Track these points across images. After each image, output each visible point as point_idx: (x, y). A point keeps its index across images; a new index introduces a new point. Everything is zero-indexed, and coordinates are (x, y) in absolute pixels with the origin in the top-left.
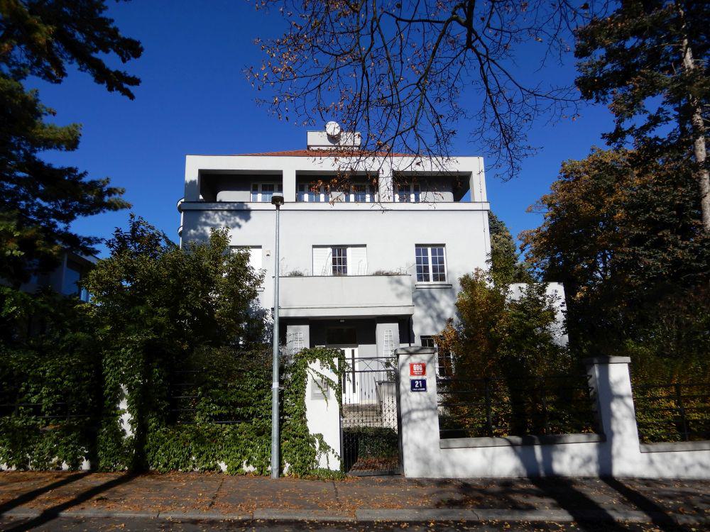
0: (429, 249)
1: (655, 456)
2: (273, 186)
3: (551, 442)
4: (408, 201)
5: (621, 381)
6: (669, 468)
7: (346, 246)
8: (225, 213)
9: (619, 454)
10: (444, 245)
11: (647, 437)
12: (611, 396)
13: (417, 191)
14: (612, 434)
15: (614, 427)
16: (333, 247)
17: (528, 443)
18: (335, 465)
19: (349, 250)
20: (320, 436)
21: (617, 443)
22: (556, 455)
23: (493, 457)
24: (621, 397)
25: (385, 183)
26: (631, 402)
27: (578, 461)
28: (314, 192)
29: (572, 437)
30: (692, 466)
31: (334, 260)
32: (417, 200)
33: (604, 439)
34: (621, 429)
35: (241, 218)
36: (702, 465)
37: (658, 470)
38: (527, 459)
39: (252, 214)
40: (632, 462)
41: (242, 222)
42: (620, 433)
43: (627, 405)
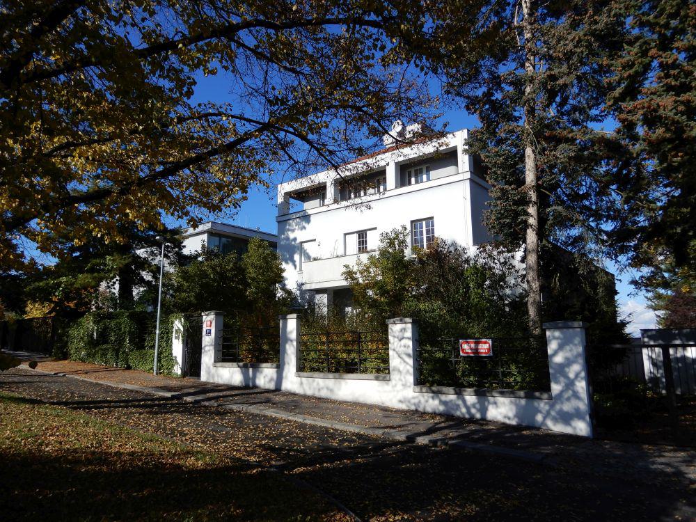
0: (424, 223)
1: (304, 380)
2: (421, 169)
3: (256, 366)
4: (422, 182)
5: (291, 332)
6: (310, 388)
7: (366, 231)
8: (298, 220)
9: (286, 376)
10: (432, 218)
11: (300, 369)
12: (287, 340)
13: (428, 170)
14: (284, 364)
15: (286, 360)
16: (357, 232)
17: (245, 366)
18: (179, 372)
19: (368, 233)
20: (176, 357)
21: (286, 368)
22: (258, 375)
23: (233, 373)
24: (291, 341)
25: (330, 192)
26: (295, 343)
27: (267, 379)
28: (418, 174)
29: (264, 365)
30: (322, 388)
31: (359, 242)
32: (428, 179)
33: (280, 368)
34: (289, 362)
35: (306, 223)
36: (328, 388)
37: (304, 390)
38: (245, 375)
39: (312, 218)
40: (292, 382)
41: (306, 225)
42: (288, 364)
43: (293, 346)
